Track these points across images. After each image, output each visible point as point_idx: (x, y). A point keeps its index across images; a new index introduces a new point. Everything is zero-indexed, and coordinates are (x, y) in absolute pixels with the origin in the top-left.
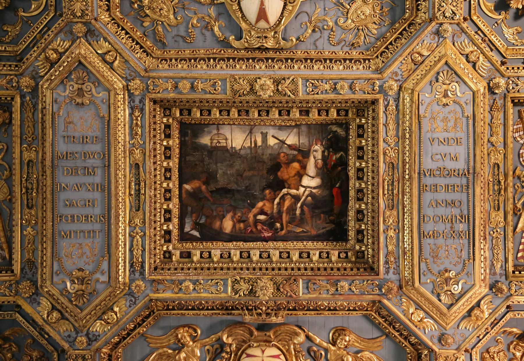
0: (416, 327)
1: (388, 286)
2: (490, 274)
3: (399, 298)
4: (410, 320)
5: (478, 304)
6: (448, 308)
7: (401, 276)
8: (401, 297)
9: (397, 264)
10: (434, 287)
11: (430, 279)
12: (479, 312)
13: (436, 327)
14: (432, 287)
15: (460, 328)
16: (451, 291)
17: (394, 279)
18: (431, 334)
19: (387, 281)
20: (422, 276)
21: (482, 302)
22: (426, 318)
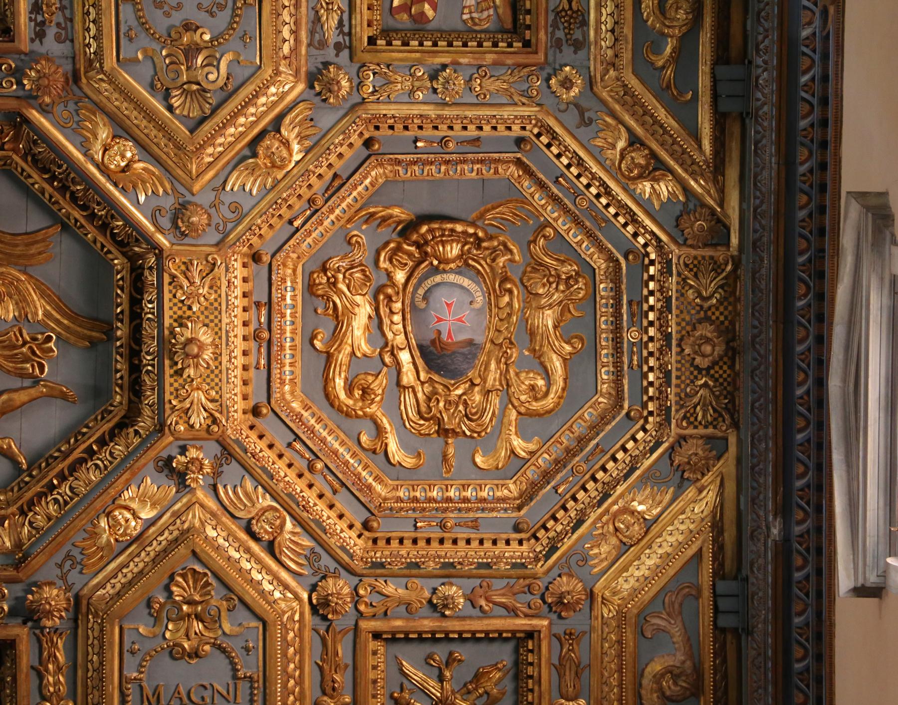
0: (116, 185)
1: (38, 71)
2: (309, 45)
3: (71, 106)
4: (102, 168)
5: (277, 124)
6: (192, 131)
7: (77, 46)
8: (76, 103)
9: (67, 13)
10: (156, 74)
11: (145, 51)
12: (277, 144)
13: (168, 186)
14: (152, 73)
15: (228, 188)
16: (198, 84)
17: (58, 53)
18: (155, 203)
19: (33, 57)
20: (123, 41)
21: (287, 120)
22: (139, 161)
